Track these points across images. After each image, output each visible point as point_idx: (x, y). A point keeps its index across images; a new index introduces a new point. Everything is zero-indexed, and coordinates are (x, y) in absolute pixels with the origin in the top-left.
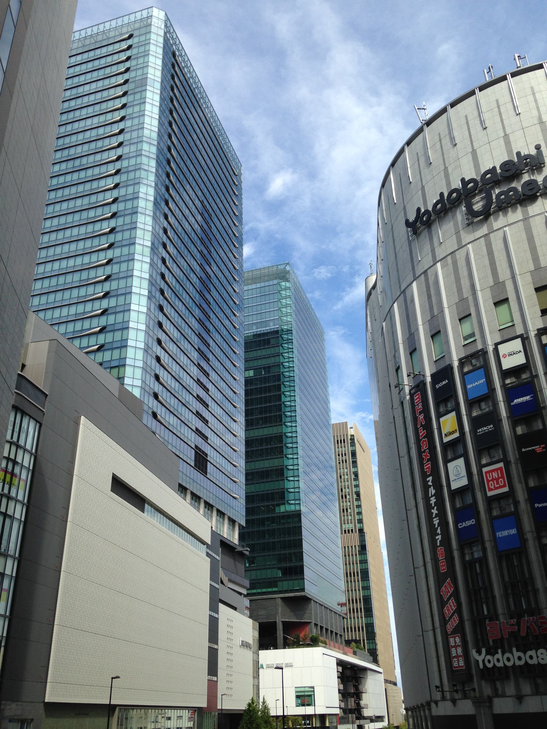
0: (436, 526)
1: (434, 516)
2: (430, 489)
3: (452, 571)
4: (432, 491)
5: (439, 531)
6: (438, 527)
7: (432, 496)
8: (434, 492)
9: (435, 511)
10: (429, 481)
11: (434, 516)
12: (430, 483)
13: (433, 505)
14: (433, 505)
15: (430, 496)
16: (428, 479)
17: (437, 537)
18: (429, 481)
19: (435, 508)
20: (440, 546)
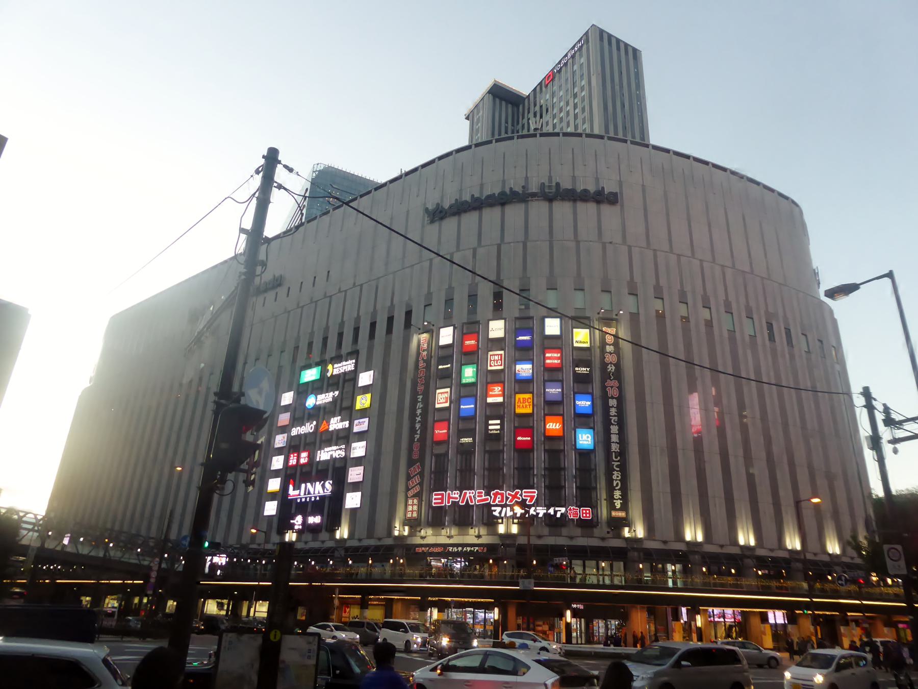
0: (417, 429)
1: (417, 422)
2: (418, 404)
3: (422, 460)
4: (420, 405)
5: (419, 432)
7: (419, 408)
9: (418, 419)
10: (419, 398)
11: (417, 422)
13: (418, 415)
14: (418, 415)
15: (417, 408)
17: (415, 436)
18: (419, 398)
19: (420, 417)
20: (417, 441)
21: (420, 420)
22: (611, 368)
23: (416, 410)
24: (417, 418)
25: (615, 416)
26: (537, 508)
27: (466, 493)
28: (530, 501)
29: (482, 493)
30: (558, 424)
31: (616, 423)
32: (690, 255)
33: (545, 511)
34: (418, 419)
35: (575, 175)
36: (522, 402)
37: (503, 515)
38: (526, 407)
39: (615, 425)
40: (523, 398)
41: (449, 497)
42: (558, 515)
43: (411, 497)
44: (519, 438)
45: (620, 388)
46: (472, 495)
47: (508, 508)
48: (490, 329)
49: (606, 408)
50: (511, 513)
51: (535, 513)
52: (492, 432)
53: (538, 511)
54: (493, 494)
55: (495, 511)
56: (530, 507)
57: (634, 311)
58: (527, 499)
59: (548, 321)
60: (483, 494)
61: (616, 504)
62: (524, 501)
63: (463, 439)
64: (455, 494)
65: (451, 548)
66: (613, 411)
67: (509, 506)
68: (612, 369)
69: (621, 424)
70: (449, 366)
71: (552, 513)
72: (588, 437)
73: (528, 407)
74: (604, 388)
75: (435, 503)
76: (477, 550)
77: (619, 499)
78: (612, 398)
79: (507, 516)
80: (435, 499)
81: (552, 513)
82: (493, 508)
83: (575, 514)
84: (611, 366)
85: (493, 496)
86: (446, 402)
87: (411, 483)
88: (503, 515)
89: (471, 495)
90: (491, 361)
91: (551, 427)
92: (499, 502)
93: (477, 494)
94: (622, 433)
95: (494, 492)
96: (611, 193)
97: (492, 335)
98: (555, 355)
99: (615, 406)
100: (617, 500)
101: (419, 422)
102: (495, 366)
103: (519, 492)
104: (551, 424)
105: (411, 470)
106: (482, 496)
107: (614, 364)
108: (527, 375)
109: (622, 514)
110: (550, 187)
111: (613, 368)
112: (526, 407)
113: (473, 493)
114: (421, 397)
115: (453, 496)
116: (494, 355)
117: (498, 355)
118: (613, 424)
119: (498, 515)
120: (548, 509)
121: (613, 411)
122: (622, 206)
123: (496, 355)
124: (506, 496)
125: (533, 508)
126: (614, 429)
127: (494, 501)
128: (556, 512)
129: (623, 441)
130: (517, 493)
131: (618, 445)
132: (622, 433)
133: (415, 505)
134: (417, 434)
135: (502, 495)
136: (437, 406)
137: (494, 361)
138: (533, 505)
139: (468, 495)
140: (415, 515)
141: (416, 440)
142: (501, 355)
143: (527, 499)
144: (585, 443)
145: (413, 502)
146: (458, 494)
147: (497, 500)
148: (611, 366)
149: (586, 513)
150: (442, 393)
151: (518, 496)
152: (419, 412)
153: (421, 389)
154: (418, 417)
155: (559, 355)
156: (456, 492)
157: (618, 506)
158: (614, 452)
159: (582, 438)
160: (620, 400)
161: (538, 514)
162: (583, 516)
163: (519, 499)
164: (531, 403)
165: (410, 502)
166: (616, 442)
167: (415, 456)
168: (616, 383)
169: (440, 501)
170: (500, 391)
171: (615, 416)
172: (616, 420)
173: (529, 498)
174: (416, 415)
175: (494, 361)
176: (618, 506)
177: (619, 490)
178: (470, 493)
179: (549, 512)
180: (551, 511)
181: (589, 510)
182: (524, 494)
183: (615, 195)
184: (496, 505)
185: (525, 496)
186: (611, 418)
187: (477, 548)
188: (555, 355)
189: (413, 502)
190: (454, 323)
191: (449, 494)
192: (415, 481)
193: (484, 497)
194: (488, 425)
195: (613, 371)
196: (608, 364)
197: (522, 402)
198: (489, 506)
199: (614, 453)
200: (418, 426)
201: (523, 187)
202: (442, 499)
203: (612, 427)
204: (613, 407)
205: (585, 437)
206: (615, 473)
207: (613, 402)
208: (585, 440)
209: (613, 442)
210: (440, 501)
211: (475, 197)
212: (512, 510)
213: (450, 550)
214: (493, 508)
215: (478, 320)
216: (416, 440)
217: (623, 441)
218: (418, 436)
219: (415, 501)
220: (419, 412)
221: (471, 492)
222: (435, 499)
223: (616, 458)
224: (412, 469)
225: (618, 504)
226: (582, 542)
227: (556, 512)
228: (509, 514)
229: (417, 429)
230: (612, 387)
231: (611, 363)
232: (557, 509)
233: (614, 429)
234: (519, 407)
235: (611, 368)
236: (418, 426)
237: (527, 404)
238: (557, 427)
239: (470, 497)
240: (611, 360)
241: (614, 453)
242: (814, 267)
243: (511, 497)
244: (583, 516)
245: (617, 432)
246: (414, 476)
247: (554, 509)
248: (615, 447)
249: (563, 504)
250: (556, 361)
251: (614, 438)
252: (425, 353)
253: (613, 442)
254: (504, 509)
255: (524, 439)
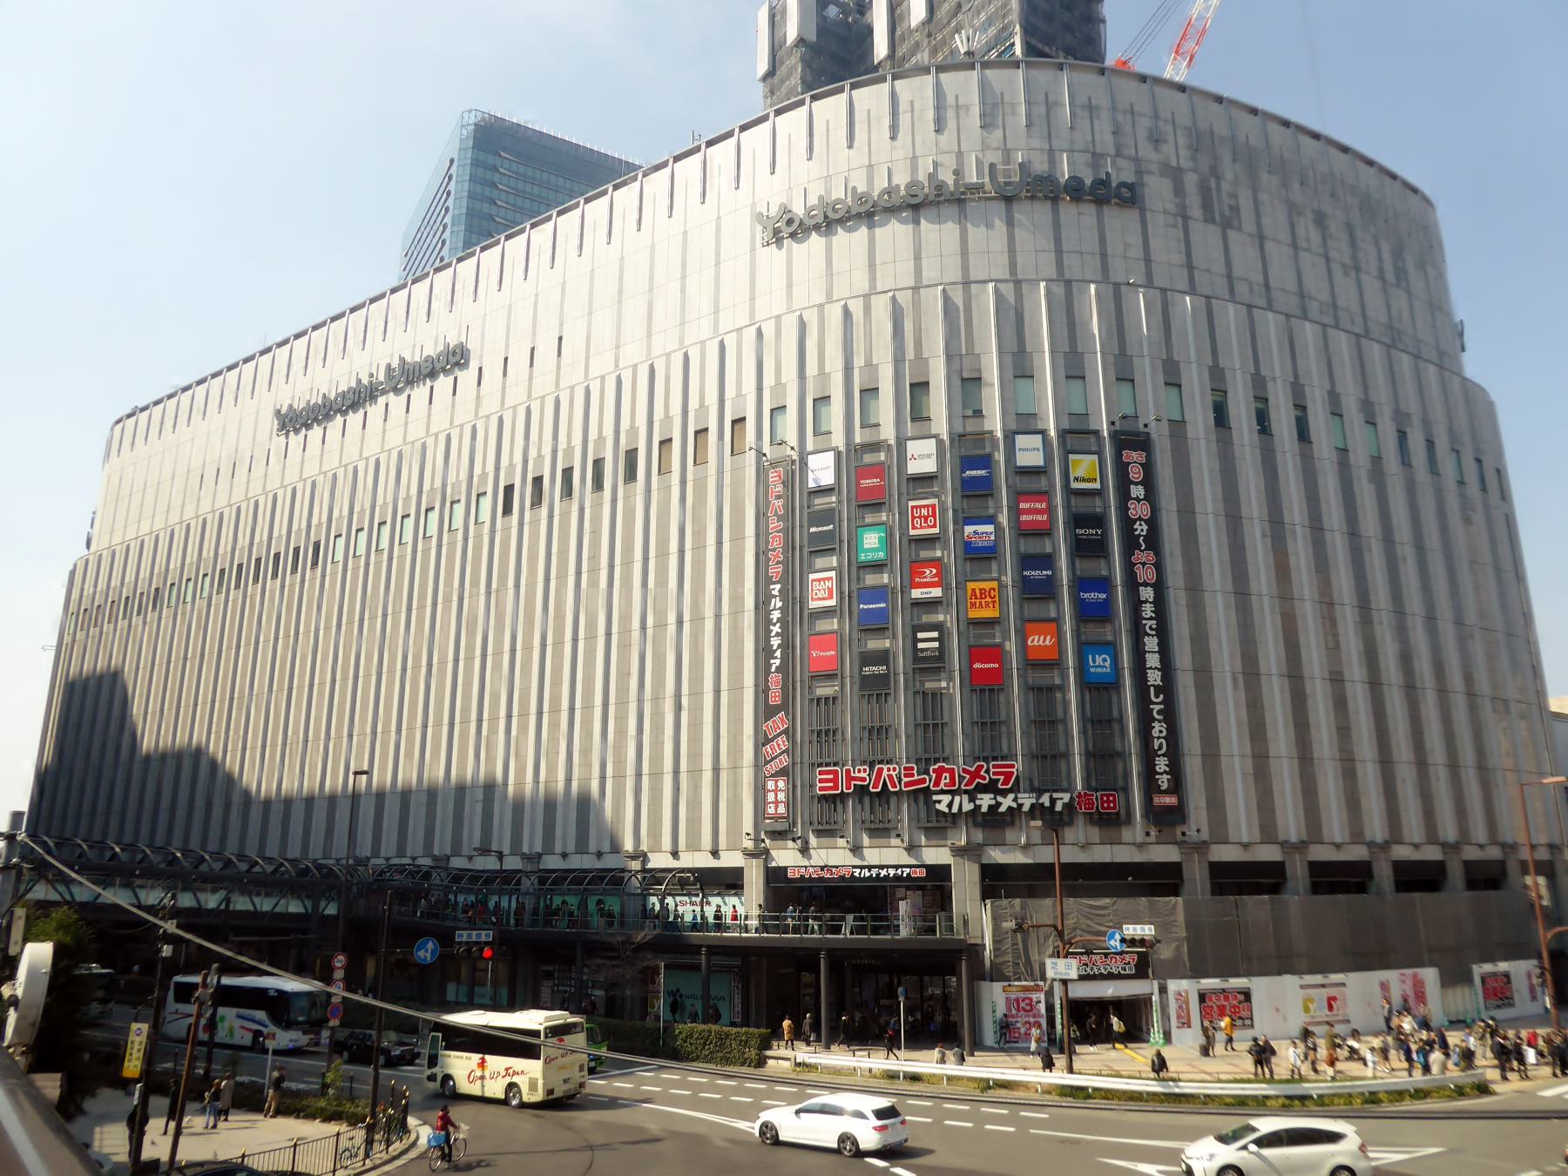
0: (775, 648)
5: (778, 654)
6: (778, 648)
8: (779, 604)
9: (776, 629)
11: (773, 634)
12: (775, 593)
13: (775, 621)
14: (775, 621)
15: (772, 607)
16: (772, 587)
17: (772, 661)
19: (778, 625)
21: (780, 631)
22: (1141, 529)
23: (769, 613)
24: (772, 627)
25: (1151, 618)
26: (1019, 795)
27: (881, 770)
28: (1006, 782)
29: (912, 769)
30: (1049, 637)
31: (1154, 633)
32: (1265, 306)
33: (1034, 801)
34: (776, 629)
35: (1054, 148)
36: (978, 596)
37: (955, 809)
38: (987, 605)
39: (1153, 636)
40: (981, 590)
41: (850, 778)
42: (1059, 807)
43: (772, 776)
44: (976, 666)
45: (1159, 566)
46: (894, 774)
47: (965, 798)
48: (909, 456)
49: (1136, 605)
50: (971, 806)
51: (1014, 805)
52: (924, 654)
53: (1020, 801)
54: (934, 771)
55: (939, 802)
56: (1004, 793)
57: (1177, 417)
58: (999, 780)
59: (1022, 441)
60: (915, 772)
61: (1160, 782)
62: (994, 782)
63: (867, 669)
64: (859, 771)
65: (858, 870)
66: (1148, 610)
67: (966, 792)
68: (1142, 530)
69: (1163, 633)
70: (831, 526)
71: (1047, 804)
72: (1104, 660)
73: (991, 605)
74: (1129, 568)
75: (821, 789)
76: (909, 874)
77: (1165, 772)
78: (1145, 584)
79: (964, 810)
80: (821, 781)
81: (1047, 804)
82: (935, 798)
83: (1089, 804)
84: (1140, 525)
85: (934, 776)
86: (830, 597)
87: (769, 750)
88: (955, 809)
89: (892, 772)
90: (913, 517)
91: (1035, 643)
92: (946, 785)
93: (903, 772)
94: (1165, 651)
95: (936, 767)
96: (1123, 184)
97: (914, 468)
98: (1038, 506)
99: (1151, 600)
100: (1161, 774)
101: (777, 634)
102: (922, 527)
103: (983, 766)
104: (1037, 637)
105: (767, 726)
106: (913, 775)
107: (1145, 521)
108: (986, 544)
109: (1170, 800)
110: (1007, 173)
111: (1145, 527)
112: (987, 605)
113: (894, 770)
114: (778, 587)
115: (857, 775)
116: (920, 507)
117: (928, 506)
118: (1149, 635)
119: (946, 810)
120: (1038, 798)
121: (1148, 610)
122: (1143, 211)
123: (924, 506)
124: (959, 776)
125: (1011, 796)
126: (1151, 643)
127: (937, 783)
128: (1053, 801)
129: (1167, 667)
130: (981, 767)
131: (1160, 673)
132: (1165, 651)
133: (781, 790)
134: (776, 658)
135: (951, 772)
136: (813, 604)
137: (920, 517)
138: (1010, 791)
139: (885, 773)
140: (782, 809)
141: (773, 669)
142: (933, 506)
143: (999, 780)
144: (1099, 670)
145: (776, 786)
146: (865, 771)
147: (943, 782)
148: (1140, 525)
149: (1108, 802)
150: (819, 580)
151: (982, 773)
152: (776, 615)
153: (777, 573)
154: (775, 625)
155: (1044, 505)
156: (862, 768)
157: (1165, 786)
158: (1153, 685)
159: (1094, 661)
160: (1159, 587)
161: (1020, 806)
162: (1103, 808)
163: (984, 778)
164: (997, 599)
165: (770, 785)
166: (1156, 668)
167: (775, 698)
168: (1149, 556)
169: (831, 784)
170: (935, 576)
171: (1151, 618)
172: (1154, 627)
173: (1002, 777)
174: (769, 622)
175: (920, 517)
176: (1165, 786)
177: (1164, 755)
178: (889, 770)
179: (1040, 801)
180: (1045, 800)
181: (1111, 795)
182: (992, 770)
183: (1130, 187)
184: (943, 792)
185: (994, 774)
186: (1144, 622)
187: (908, 870)
188: (1038, 506)
189: (776, 786)
190: (833, 445)
191: (848, 771)
192: (778, 745)
193: (916, 777)
194: (916, 641)
195: (1144, 533)
196: (1135, 521)
197: (978, 596)
198: (927, 792)
199: (1152, 688)
200: (775, 642)
201: (956, 173)
202: (835, 781)
203: (1146, 639)
204: (1146, 602)
205: (1099, 660)
206: (1156, 724)
207: (1147, 593)
208: (1100, 666)
209: (1151, 668)
210: (831, 784)
211: (859, 191)
212: (972, 800)
213: (857, 874)
214: (935, 798)
215: (882, 438)
216: (773, 669)
217: (1167, 667)
218: (778, 662)
219: (781, 784)
220: (776, 615)
221: (891, 767)
222: (821, 781)
223: (1157, 697)
224: (770, 723)
225: (1164, 781)
226: (1103, 854)
227: (1053, 801)
228: (968, 807)
229: (775, 648)
230: (1144, 564)
231: (1140, 519)
232: (1055, 795)
233: (1151, 643)
234: (973, 605)
235: (1141, 529)
236: (775, 642)
237: (988, 599)
238: (1047, 643)
239: (890, 777)
240: (1139, 512)
241: (1152, 688)
242: (1457, 319)
243: (968, 777)
244: (1103, 808)
245: (1157, 649)
246: (775, 737)
247: (1051, 798)
248: (1154, 678)
249: (1065, 784)
250: (1039, 518)
251: (1153, 660)
252: (779, 503)
253: (1151, 668)
254: (957, 799)
255: (987, 666)
